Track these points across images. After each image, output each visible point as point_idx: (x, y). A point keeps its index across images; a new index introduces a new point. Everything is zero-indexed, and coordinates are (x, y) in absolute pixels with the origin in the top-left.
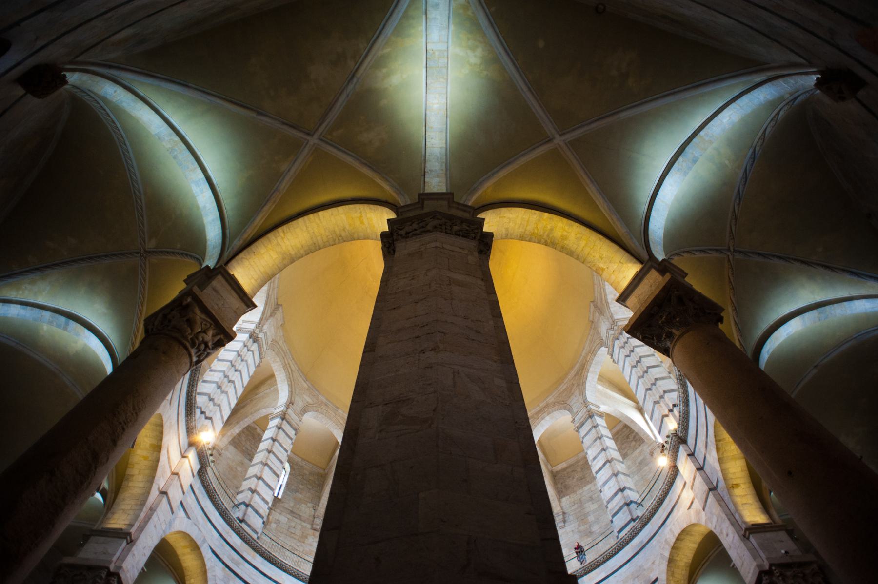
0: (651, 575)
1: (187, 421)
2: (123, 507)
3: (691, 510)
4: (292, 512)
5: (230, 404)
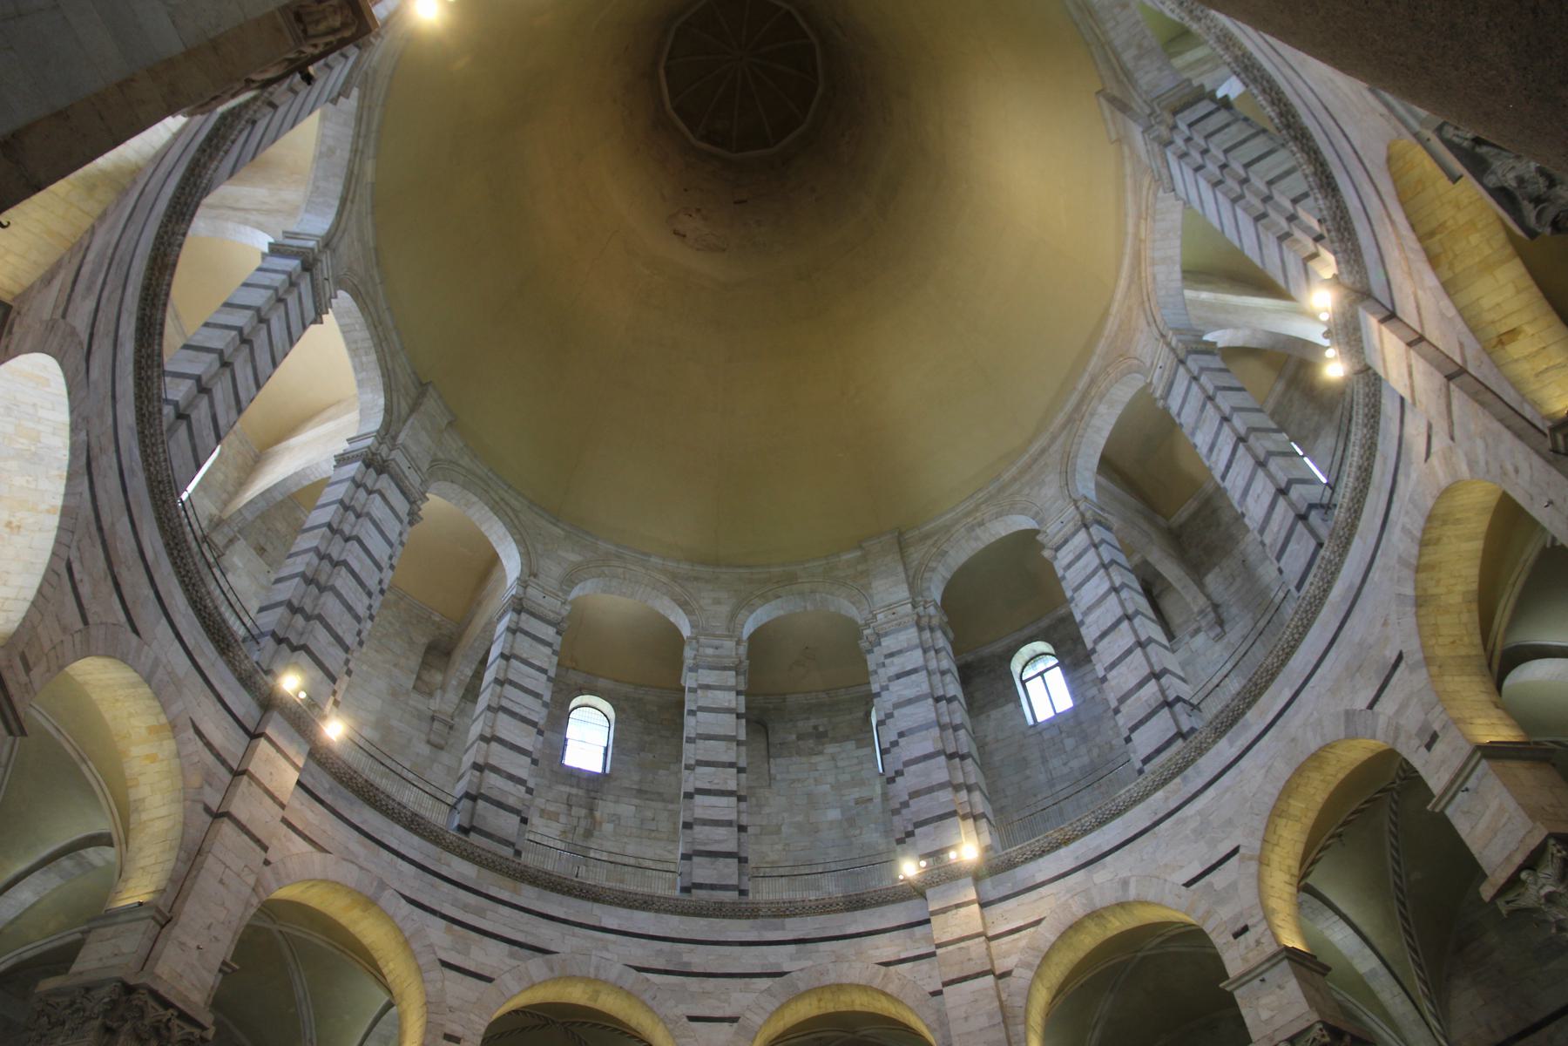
0: (1387, 653)
1: (231, 663)
2: (142, 863)
3: (1434, 459)
4: (640, 791)
5: (350, 609)
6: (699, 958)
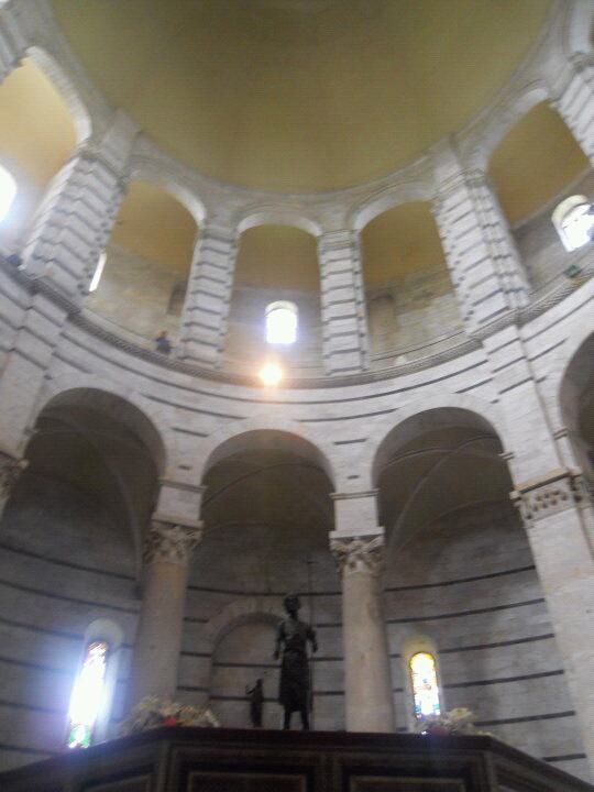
6: (339, 410)
